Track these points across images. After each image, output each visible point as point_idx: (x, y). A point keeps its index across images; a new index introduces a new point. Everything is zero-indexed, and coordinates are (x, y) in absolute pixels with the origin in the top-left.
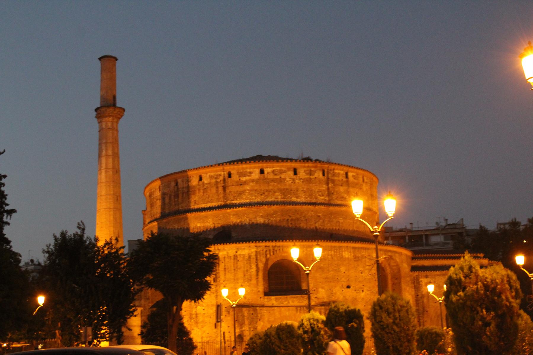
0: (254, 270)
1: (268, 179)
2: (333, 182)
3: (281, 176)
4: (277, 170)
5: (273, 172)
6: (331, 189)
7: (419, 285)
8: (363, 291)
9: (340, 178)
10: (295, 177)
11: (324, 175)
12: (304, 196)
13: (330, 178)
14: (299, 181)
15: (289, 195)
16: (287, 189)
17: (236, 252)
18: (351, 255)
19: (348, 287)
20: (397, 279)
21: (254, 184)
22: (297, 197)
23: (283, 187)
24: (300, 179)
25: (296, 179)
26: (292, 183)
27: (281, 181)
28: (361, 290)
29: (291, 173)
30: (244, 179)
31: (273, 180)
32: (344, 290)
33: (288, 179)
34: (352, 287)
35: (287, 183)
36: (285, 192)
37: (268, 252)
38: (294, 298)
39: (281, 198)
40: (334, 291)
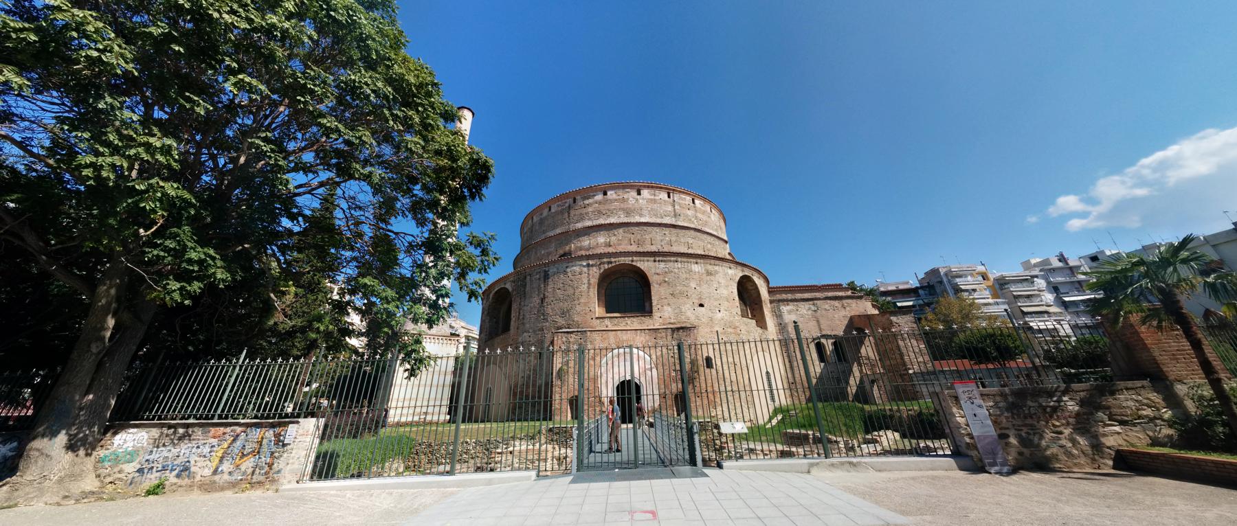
0: (586, 285)
2: (679, 204)
6: (677, 211)
9: (687, 203)
10: (638, 197)
11: (669, 197)
17: (567, 267)
19: (701, 305)
21: (597, 205)
22: (641, 215)
24: (643, 199)
29: (634, 193)
30: (587, 202)
33: (631, 199)
34: (705, 306)
36: (628, 212)
40: (683, 310)
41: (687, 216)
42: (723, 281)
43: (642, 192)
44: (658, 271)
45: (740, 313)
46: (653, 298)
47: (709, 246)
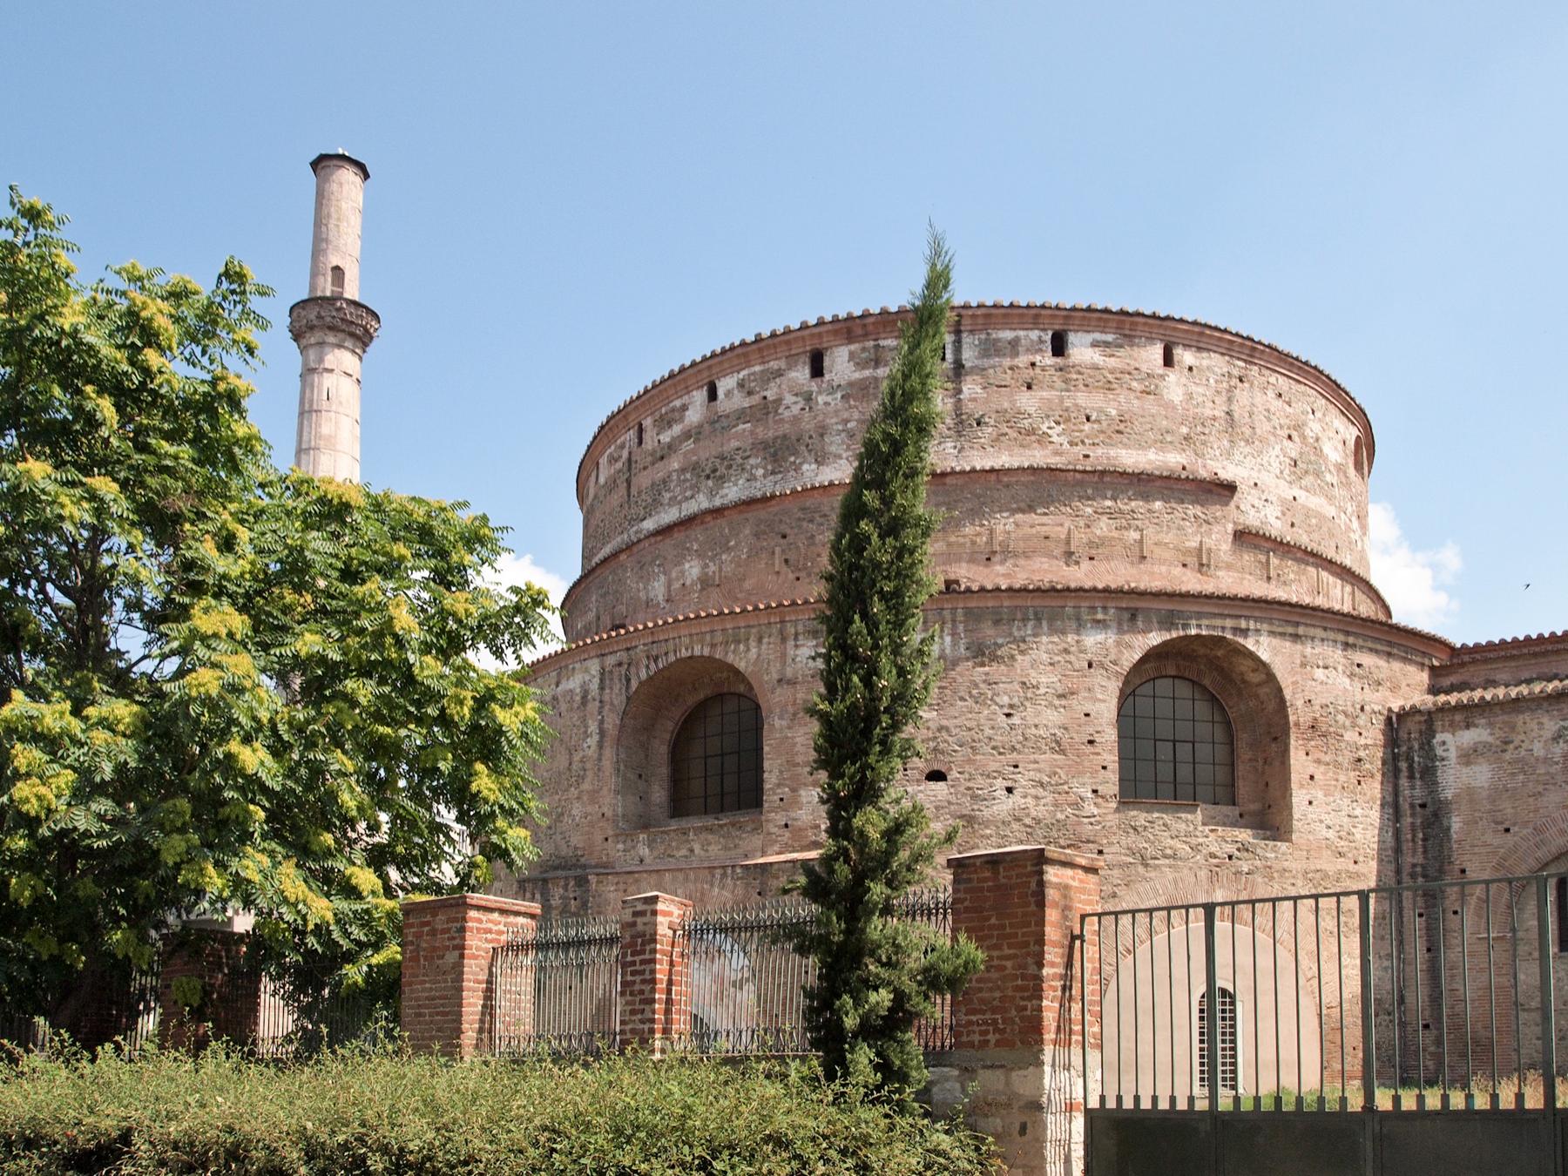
1: (727, 416)
3: (765, 393)
4: (753, 374)
5: (741, 385)
6: (969, 407)
7: (1434, 758)
8: (1010, 790)
12: (848, 449)
13: (968, 364)
14: (829, 399)
15: (792, 459)
16: (785, 437)
18: (954, 644)
20: (1275, 739)
23: (771, 434)
24: (833, 389)
25: (820, 393)
26: (803, 409)
27: (767, 409)
28: (1000, 783)
29: (801, 374)
31: (742, 415)
32: (909, 789)
33: (789, 399)
34: (953, 775)
35: (787, 414)
37: (633, 670)
38: (710, 830)
39: (765, 476)
41: (1010, 418)
42: (1047, 680)
43: (827, 362)
44: (789, 672)
45: (1116, 789)
46: (766, 765)
47: (1103, 527)
